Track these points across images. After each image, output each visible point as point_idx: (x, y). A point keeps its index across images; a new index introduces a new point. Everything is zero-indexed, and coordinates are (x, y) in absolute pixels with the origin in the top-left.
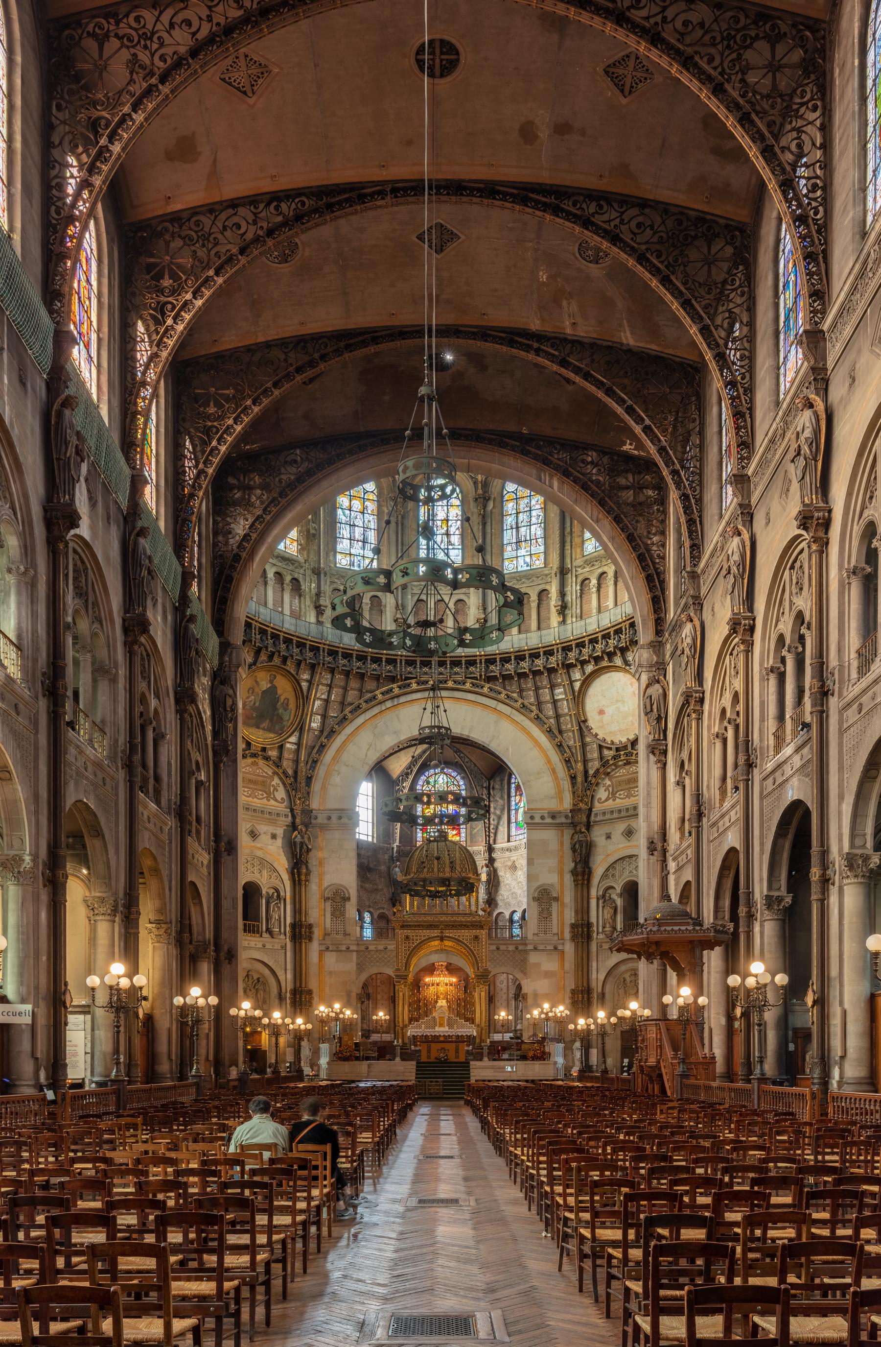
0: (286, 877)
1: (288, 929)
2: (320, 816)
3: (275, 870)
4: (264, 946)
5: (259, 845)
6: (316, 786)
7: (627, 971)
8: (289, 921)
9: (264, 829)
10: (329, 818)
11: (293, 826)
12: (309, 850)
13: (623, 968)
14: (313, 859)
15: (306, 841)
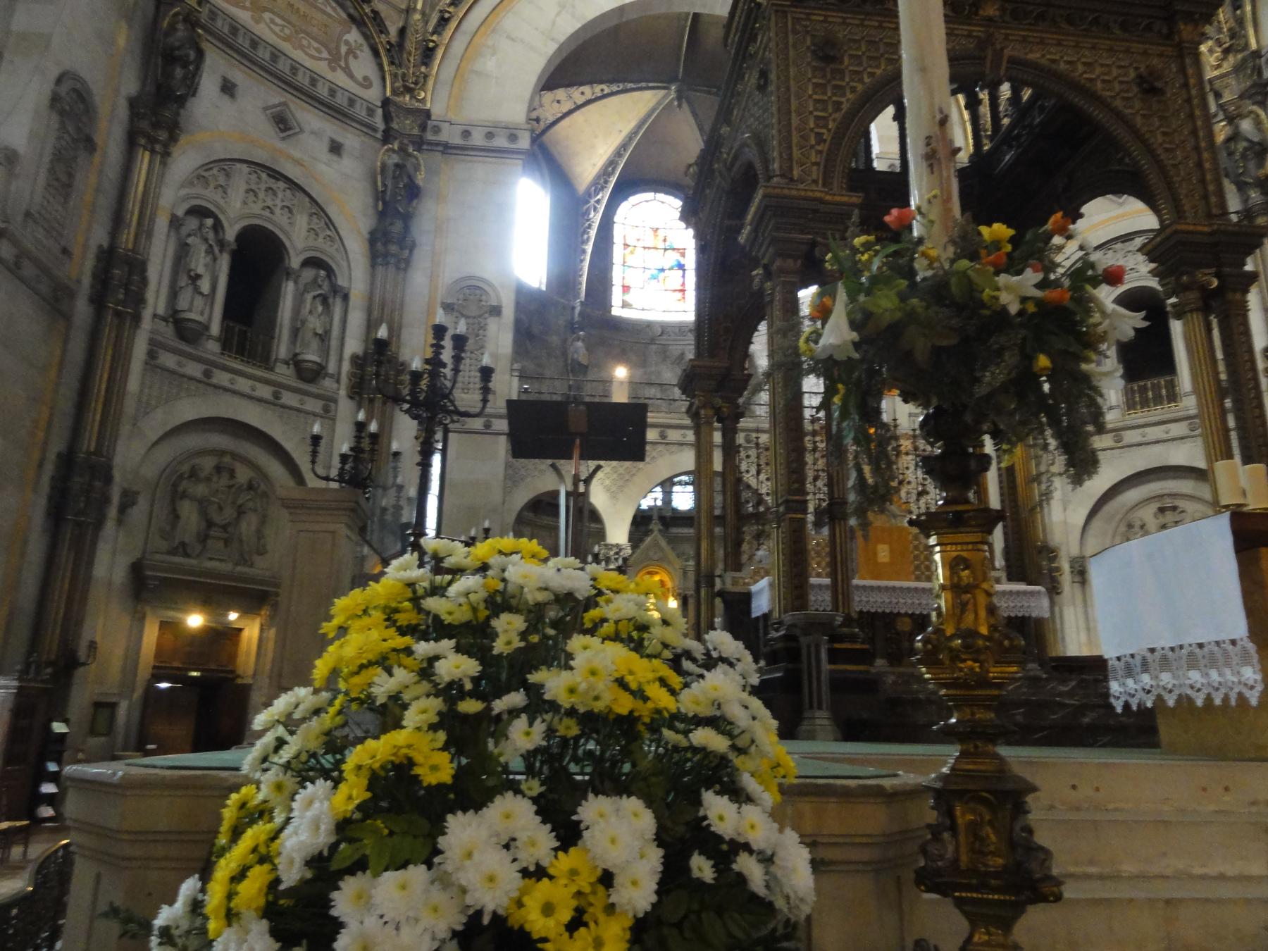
0: (356, 247)
1: (346, 366)
2: (445, 126)
3: (330, 223)
4: (277, 396)
5: (296, 154)
6: (443, 68)
7: (1148, 500)
8: (354, 346)
9: (308, 118)
10: (466, 134)
11: (387, 137)
12: (414, 192)
13: (1132, 495)
14: (428, 214)
15: (410, 167)
